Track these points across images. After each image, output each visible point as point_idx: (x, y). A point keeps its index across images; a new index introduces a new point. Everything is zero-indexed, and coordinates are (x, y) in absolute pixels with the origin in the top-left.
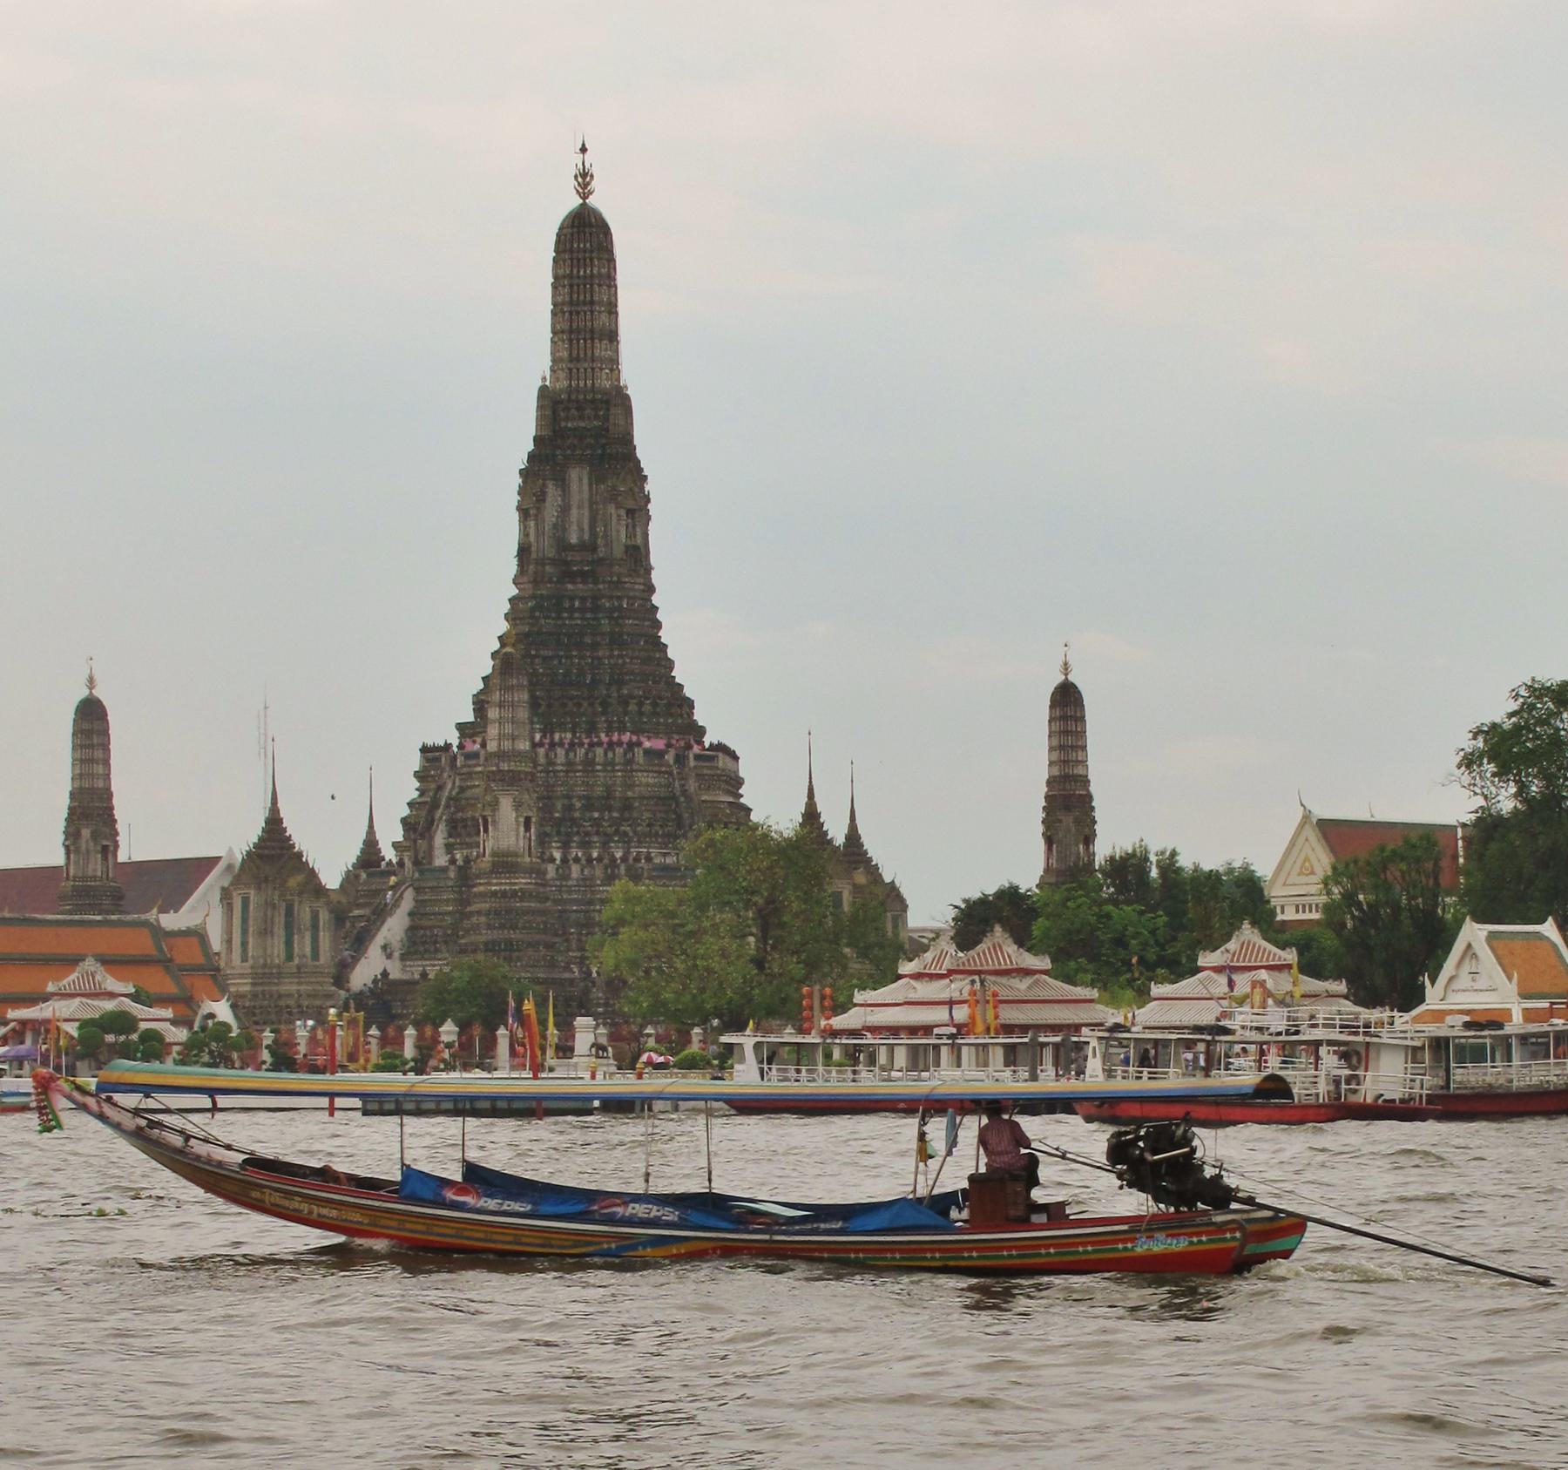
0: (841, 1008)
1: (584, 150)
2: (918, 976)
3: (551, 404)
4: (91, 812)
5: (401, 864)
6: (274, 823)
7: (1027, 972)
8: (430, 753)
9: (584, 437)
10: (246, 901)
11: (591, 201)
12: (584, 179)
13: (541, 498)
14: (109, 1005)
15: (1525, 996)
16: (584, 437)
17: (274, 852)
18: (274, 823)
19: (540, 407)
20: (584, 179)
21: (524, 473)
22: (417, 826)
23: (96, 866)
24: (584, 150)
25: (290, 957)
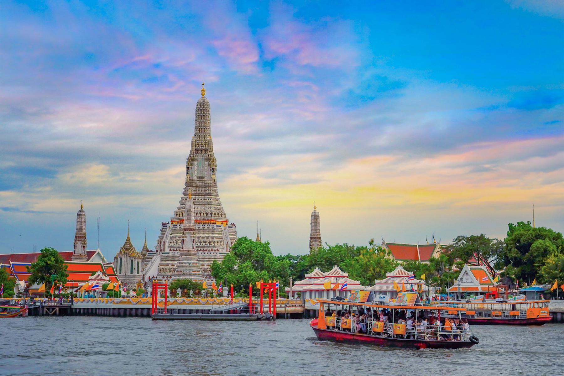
0: (293, 284)
2: (311, 278)
3: (195, 144)
4: (80, 237)
5: (157, 251)
6: (128, 240)
7: (343, 277)
8: (165, 225)
9: (202, 151)
10: (121, 259)
14: (104, 283)
15: (481, 284)
16: (202, 151)
17: (127, 248)
18: (128, 240)
19: (192, 144)
21: (188, 159)
22: (160, 242)
23: (79, 250)
25: (132, 273)
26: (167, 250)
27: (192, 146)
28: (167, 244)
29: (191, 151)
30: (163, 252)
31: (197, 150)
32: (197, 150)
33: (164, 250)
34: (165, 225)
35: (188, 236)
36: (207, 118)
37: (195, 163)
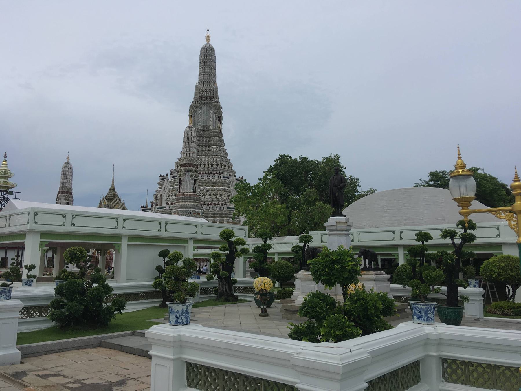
1: (208, 30)
3: (198, 90)
6: (113, 190)
8: (162, 178)
11: (210, 43)
12: (208, 38)
13: (195, 112)
18: (113, 190)
19: (196, 90)
20: (208, 38)
24: (208, 30)
26: (164, 204)
27: (196, 93)
28: (164, 198)
29: (194, 98)
30: (159, 206)
31: (201, 97)
32: (201, 97)
33: (161, 205)
34: (162, 178)
35: (188, 175)
36: (212, 64)
37: (199, 111)
